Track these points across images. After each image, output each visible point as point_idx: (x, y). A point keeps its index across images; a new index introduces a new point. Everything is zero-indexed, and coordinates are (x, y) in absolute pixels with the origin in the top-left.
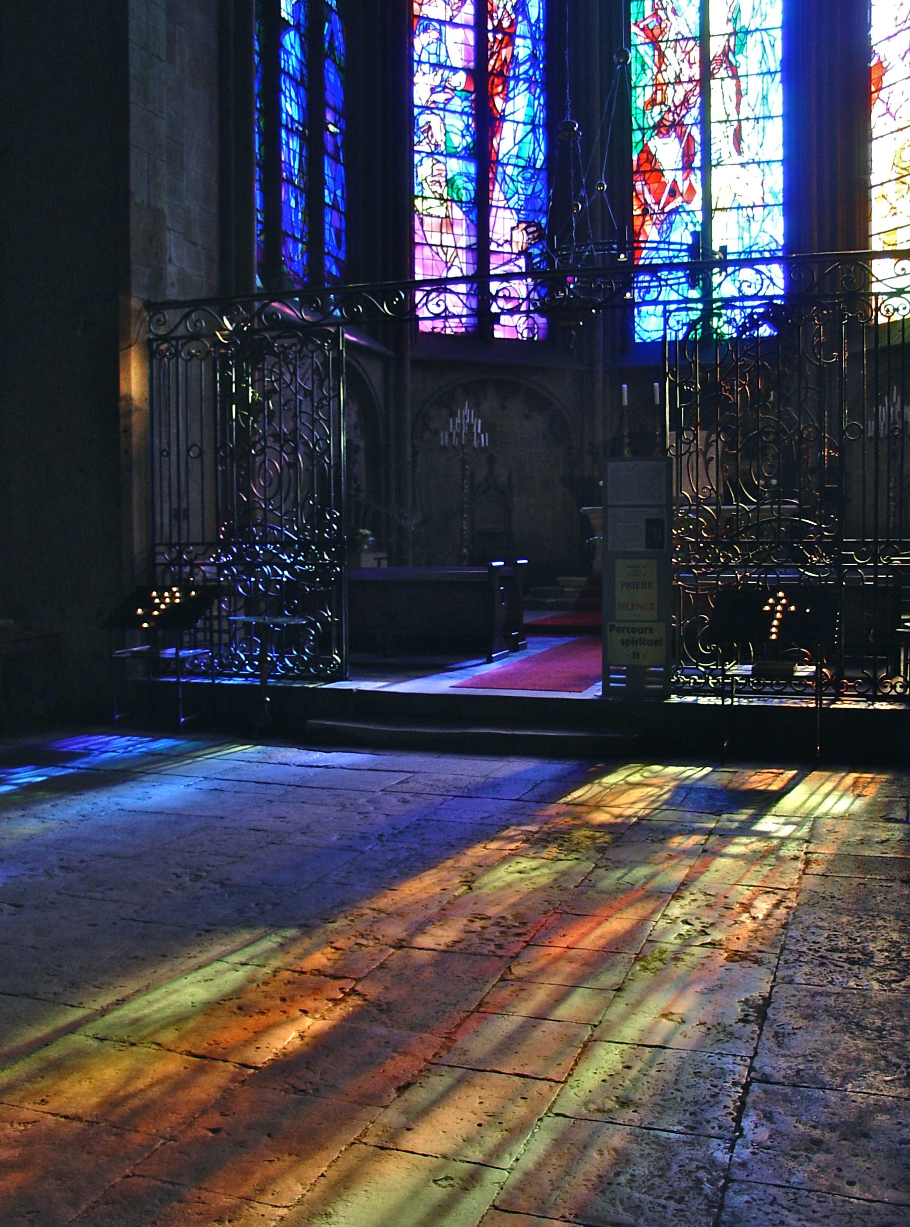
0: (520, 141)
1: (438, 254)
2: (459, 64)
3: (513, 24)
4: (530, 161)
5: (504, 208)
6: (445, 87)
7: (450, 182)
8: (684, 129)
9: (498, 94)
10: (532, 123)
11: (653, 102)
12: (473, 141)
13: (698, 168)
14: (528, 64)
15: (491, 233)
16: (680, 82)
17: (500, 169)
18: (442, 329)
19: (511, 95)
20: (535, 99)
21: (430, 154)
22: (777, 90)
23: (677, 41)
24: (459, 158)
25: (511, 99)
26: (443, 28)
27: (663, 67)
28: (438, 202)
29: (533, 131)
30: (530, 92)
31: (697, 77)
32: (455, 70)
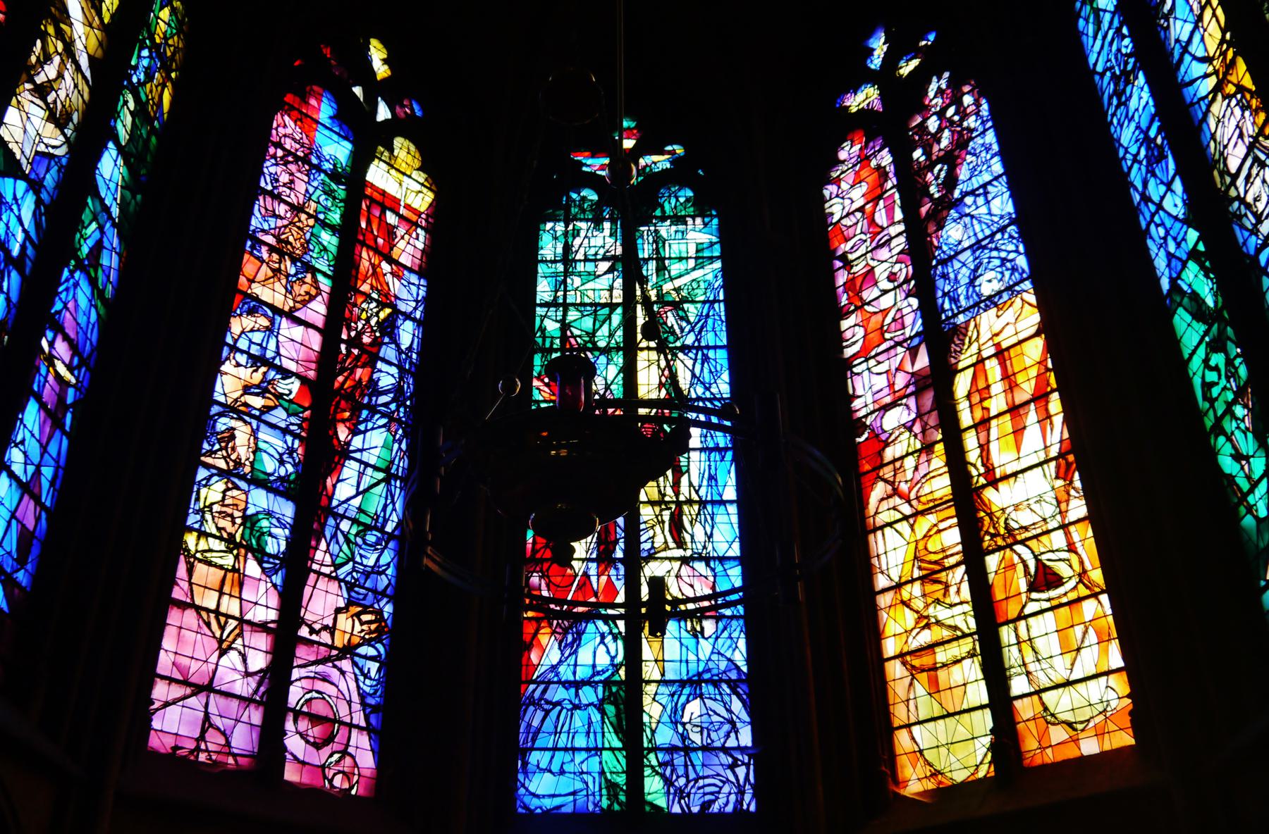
1: (208, 625)
2: (292, 366)
3: (377, 343)
4: (377, 521)
5: (329, 576)
9: (343, 421)
10: (386, 470)
12: (296, 472)
13: (620, 560)
14: (392, 395)
15: (303, 611)
17: (331, 521)
18: (192, 752)
19: (362, 427)
20: (394, 441)
21: (222, 473)
22: (729, 472)
24: (269, 490)
25: (360, 432)
26: (278, 318)
28: (221, 546)
29: (387, 480)
30: (389, 430)
32: (286, 374)
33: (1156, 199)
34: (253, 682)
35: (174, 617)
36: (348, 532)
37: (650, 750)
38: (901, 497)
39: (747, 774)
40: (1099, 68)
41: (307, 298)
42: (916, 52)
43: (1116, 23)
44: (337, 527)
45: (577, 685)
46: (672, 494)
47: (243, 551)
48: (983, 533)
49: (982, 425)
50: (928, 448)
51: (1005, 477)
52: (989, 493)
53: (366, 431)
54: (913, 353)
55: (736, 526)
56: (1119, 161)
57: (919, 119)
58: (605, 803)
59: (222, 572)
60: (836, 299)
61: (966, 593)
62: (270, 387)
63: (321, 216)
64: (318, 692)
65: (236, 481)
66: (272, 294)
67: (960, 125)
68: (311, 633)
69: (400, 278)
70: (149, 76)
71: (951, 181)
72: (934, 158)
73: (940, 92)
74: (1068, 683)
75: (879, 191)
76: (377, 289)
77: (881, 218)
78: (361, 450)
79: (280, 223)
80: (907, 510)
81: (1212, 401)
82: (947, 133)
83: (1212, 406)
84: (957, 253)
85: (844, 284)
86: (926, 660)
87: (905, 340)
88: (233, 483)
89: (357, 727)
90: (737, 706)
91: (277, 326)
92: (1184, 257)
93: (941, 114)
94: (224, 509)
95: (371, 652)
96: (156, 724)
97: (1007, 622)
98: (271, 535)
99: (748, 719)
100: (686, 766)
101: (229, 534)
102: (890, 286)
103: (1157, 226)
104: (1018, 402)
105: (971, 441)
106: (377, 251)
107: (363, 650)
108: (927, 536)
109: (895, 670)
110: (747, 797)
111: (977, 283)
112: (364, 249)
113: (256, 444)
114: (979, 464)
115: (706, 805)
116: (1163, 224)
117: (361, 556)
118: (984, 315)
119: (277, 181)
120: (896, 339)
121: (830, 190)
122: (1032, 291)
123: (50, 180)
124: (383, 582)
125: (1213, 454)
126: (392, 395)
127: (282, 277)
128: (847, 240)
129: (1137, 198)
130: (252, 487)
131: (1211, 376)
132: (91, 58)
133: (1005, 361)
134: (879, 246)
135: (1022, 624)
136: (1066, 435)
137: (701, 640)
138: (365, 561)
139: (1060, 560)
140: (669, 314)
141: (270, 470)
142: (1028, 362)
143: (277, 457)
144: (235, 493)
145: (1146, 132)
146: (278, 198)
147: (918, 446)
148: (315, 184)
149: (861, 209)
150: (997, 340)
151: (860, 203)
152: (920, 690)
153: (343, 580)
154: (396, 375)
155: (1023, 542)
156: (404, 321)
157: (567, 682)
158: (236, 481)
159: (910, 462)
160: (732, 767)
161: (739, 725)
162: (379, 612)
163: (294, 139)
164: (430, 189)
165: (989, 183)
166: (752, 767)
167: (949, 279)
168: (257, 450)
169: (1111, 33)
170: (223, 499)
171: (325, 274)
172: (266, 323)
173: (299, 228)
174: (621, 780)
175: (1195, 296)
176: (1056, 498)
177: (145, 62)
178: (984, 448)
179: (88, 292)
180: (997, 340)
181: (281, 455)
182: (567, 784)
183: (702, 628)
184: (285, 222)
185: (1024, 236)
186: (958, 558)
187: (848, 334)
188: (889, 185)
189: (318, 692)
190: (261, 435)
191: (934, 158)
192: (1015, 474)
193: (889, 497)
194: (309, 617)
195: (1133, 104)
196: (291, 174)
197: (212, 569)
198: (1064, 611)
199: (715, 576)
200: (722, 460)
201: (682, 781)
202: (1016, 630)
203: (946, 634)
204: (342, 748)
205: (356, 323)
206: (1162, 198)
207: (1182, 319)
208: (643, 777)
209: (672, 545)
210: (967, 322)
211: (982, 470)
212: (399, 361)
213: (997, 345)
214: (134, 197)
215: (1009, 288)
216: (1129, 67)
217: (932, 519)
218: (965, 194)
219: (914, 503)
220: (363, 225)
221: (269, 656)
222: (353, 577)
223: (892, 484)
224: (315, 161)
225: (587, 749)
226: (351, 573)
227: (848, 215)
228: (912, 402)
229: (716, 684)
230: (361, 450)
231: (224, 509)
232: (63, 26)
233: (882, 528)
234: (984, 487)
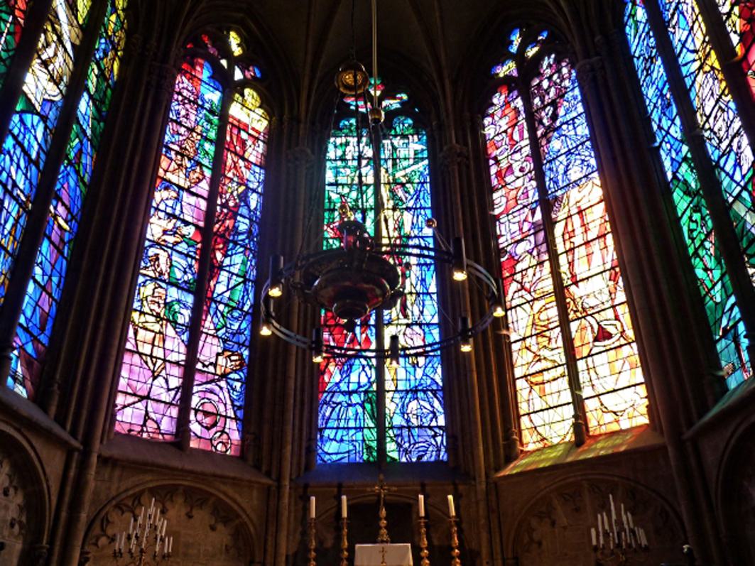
1: (146, 363)
2: (189, 219)
3: (238, 206)
5: (213, 336)
6: (176, 233)
9: (219, 249)
10: (244, 277)
13: (373, 325)
17: (213, 305)
18: (139, 432)
19: (230, 253)
20: (248, 260)
21: (152, 279)
26: (181, 192)
28: (153, 319)
29: (244, 282)
30: (245, 255)
32: (187, 223)
33: (666, 128)
34: (173, 393)
35: (127, 358)
37: (390, 428)
38: (526, 290)
39: (442, 440)
40: (637, 55)
42: (535, 42)
43: (646, 29)
44: (217, 308)
45: (350, 393)
51: (582, 280)
53: (232, 255)
56: (645, 107)
58: (365, 457)
59: (153, 334)
60: (490, 181)
61: (560, 343)
63: (204, 134)
64: (208, 399)
66: (178, 178)
69: (249, 169)
70: (106, 55)
71: (554, 117)
72: (546, 103)
73: (550, 66)
74: (614, 391)
75: (515, 121)
77: (516, 137)
78: (230, 266)
79: (181, 138)
80: (529, 298)
81: (693, 239)
82: (553, 90)
83: (693, 242)
84: (558, 157)
85: (496, 174)
86: (538, 379)
89: (230, 417)
90: (436, 404)
92: (680, 160)
93: (550, 78)
95: (237, 376)
96: (119, 418)
97: (582, 358)
98: (180, 313)
99: (442, 411)
100: (409, 436)
103: (666, 143)
105: (563, 260)
106: (236, 154)
107: (232, 376)
108: (540, 312)
109: (521, 384)
110: (442, 453)
111: (568, 173)
113: (171, 263)
114: (568, 273)
115: (420, 457)
116: (669, 142)
117: (231, 324)
119: (179, 114)
121: (487, 121)
122: (598, 178)
123: (52, 115)
125: (692, 268)
128: (497, 148)
129: (655, 127)
131: (693, 226)
132: (73, 45)
134: (515, 152)
135: (590, 359)
136: (615, 257)
137: (418, 369)
138: (233, 327)
140: (400, 190)
141: (179, 277)
144: (159, 290)
145: (661, 91)
146: (180, 124)
148: (201, 115)
149: (505, 131)
150: (578, 205)
151: (504, 128)
152: (536, 393)
153: (221, 338)
155: (591, 315)
157: (345, 391)
159: (531, 272)
160: (434, 437)
161: (438, 414)
162: (241, 355)
163: (188, 90)
164: (265, 119)
165: (576, 117)
166: (445, 437)
168: (171, 266)
169: (644, 34)
170: (153, 293)
171: (207, 167)
172: (175, 195)
174: (374, 444)
175: (685, 182)
177: (103, 46)
178: (571, 264)
179: (75, 178)
180: (578, 205)
181: (185, 269)
182: (345, 447)
183: (418, 363)
184: (184, 138)
185: (595, 147)
186: (557, 324)
187: (496, 202)
188: (520, 118)
189: (208, 399)
191: (546, 103)
192: (587, 278)
193: (519, 290)
194: (202, 358)
195: (655, 75)
196: (187, 110)
197: (148, 332)
198: (613, 352)
199: (425, 333)
200: (428, 270)
201: (407, 445)
202: (587, 362)
203: (550, 365)
204: (221, 429)
206: (669, 128)
207: (677, 195)
208: (386, 443)
209: (401, 316)
210: (563, 194)
211: (570, 276)
214: (99, 124)
215: (586, 176)
216: (653, 54)
217: (542, 302)
218: (563, 124)
219: (533, 294)
220: (228, 138)
221: (181, 380)
223: (521, 283)
224: (200, 102)
225: (355, 428)
227: (498, 134)
228: (532, 238)
229: (425, 392)
230: (230, 266)
232: (56, 26)
233: (515, 307)
234: (570, 285)
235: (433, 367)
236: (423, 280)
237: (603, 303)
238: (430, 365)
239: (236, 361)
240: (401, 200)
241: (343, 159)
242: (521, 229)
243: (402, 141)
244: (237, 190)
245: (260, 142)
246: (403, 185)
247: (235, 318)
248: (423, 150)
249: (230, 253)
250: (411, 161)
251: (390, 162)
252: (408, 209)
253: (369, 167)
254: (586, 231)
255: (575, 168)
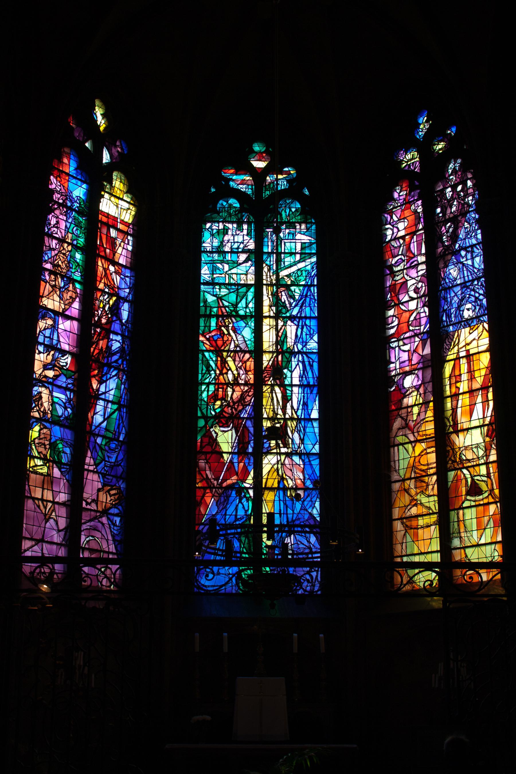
0: (109, 417)
1: (39, 507)
2: (66, 347)
4: (115, 434)
5: (93, 471)
7: (53, 446)
8: (240, 421)
9: (94, 376)
11: (214, 397)
14: (118, 355)
16: (239, 385)
19: (104, 379)
20: (122, 384)
23: (235, 352)
24: (61, 426)
27: (225, 371)
30: (118, 378)
31: (252, 381)
32: (64, 353)
36: (101, 444)
41: (71, 301)
46: (282, 414)
47: (51, 464)
48: (448, 459)
49: (455, 396)
50: (426, 403)
51: (463, 430)
52: (454, 437)
53: (107, 380)
54: (424, 342)
55: (317, 434)
57: (441, 187)
59: (43, 477)
62: (56, 363)
65: (45, 424)
67: (464, 200)
68: (86, 505)
71: (454, 237)
73: (454, 172)
75: (413, 229)
76: (108, 285)
77: (414, 247)
84: (453, 286)
87: (420, 334)
88: (43, 425)
91: (57, 322)
93: (454, 188)
94: (41, 441)
98: (64, 452)
101: (44, 455)
102: (414, 295)
104: (474, 388)
106: (105, 258)
107: (112, 511)
112: (99, 259)
113: (52, 400)
114: (451, 419)
117: (108, 457)
118: (463, 330)
120: (415, 332)
124: (120, 470)
126: (118, 355)
127: (57, 290)
130: (53, 426)
133: (470, 361)
134: (411, 267)
135: (461, 512)
139: (482, 481)
141: (60, 414)
142: (482, 366)
143: (63, 404)
144: (45, 431)
147: (421, 401)
149: (403, 237)
150: (468, 348)
151: (402, 233)
154: (121, 341)
155: (467, 468)
156: (124, 303)
158: (45, 424)
167: (447, 301)
168: (53, 403)
171: (79, 282)
173: (64, 254)
176: (485, 447)
180: (468, 348)
181: (65, 403)
190: (55, 394)
191: (447, 217)
192: (467, 429)
197: (38, 476)
198: (481, 508)
199: (304, 465)
200: (311, 392)
202: (458, 514)
205: (98, 311)
212: (122, 331)
213: (468, 351)
218: (461, 248)
219: (416, 434)
222: (105, 470)
226: (104, 468)
228: (420, 374)
231: (41, 441)
233: (398, 445)
234: (452, 433)
235: (311, 501)
236: (305, 404)
237: (478, 458)
238: (309, 499)
239: (114, 495)
240: (285, 307)
241: (219, 251)
242: (410, 360)
243: (287, 231)
244: (109, 301)
245: (129, 238)
246: (287, 287)
247: (112, 450)
248: (311, 244)
249: (104, 379)
250: (298, 257)
251: (274, 257)
252: (292, 318)
253: (250, 262)
254: (471, 379)
255: (469, 306)
